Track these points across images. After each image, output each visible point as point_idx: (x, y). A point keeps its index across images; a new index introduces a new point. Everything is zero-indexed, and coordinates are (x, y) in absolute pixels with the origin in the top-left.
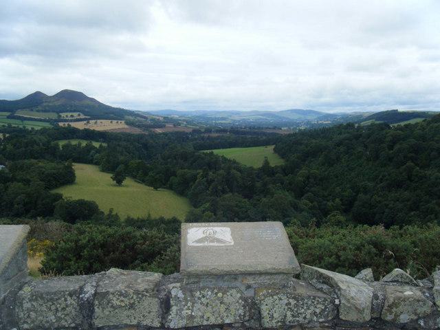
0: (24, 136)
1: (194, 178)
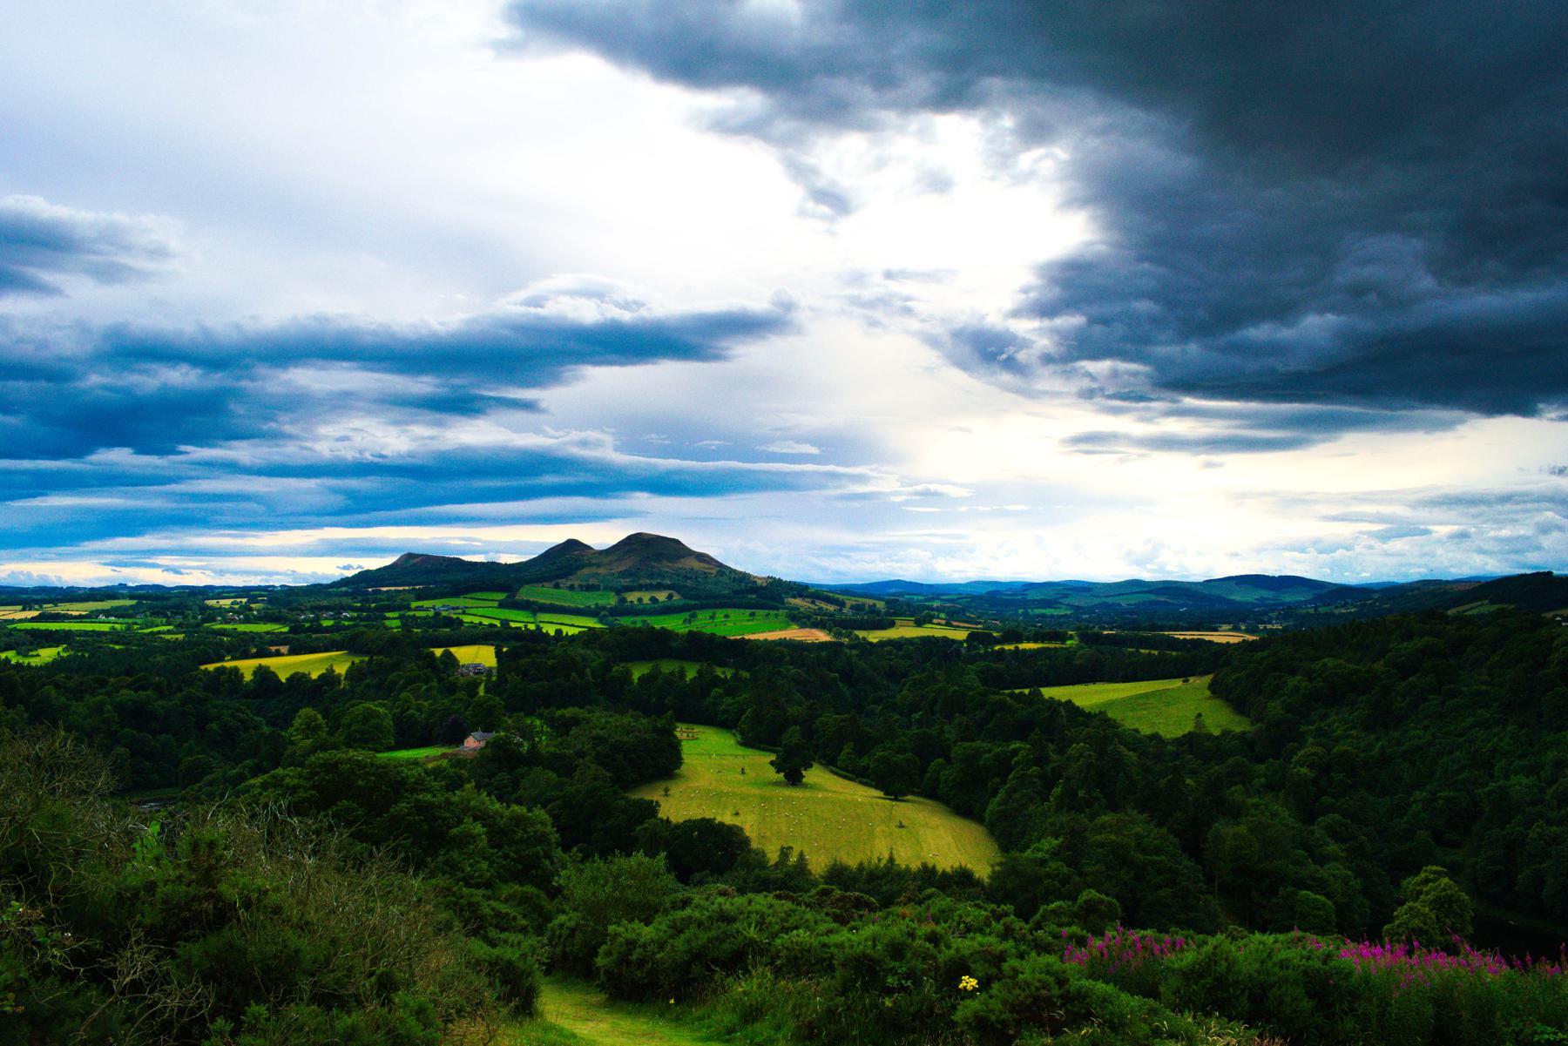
0: (545, 651)
1: (1003, 766)
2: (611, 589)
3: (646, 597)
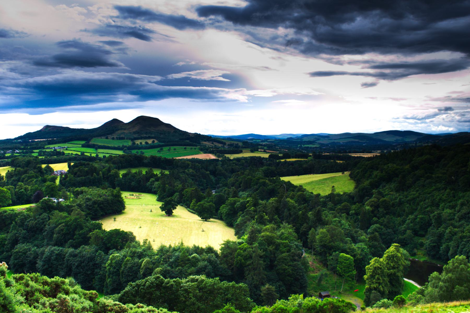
2: (130, 139)
3: (143, 142)
